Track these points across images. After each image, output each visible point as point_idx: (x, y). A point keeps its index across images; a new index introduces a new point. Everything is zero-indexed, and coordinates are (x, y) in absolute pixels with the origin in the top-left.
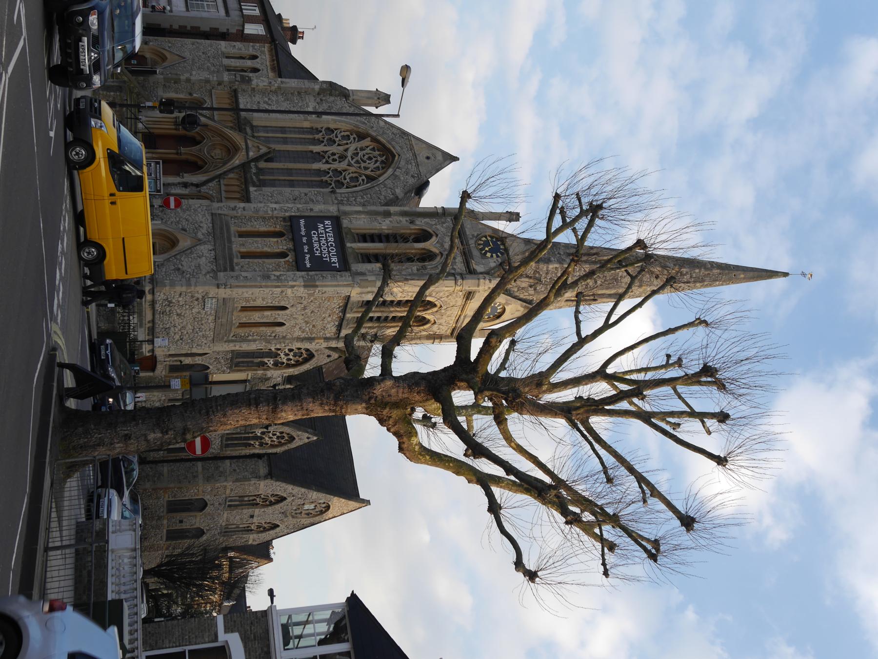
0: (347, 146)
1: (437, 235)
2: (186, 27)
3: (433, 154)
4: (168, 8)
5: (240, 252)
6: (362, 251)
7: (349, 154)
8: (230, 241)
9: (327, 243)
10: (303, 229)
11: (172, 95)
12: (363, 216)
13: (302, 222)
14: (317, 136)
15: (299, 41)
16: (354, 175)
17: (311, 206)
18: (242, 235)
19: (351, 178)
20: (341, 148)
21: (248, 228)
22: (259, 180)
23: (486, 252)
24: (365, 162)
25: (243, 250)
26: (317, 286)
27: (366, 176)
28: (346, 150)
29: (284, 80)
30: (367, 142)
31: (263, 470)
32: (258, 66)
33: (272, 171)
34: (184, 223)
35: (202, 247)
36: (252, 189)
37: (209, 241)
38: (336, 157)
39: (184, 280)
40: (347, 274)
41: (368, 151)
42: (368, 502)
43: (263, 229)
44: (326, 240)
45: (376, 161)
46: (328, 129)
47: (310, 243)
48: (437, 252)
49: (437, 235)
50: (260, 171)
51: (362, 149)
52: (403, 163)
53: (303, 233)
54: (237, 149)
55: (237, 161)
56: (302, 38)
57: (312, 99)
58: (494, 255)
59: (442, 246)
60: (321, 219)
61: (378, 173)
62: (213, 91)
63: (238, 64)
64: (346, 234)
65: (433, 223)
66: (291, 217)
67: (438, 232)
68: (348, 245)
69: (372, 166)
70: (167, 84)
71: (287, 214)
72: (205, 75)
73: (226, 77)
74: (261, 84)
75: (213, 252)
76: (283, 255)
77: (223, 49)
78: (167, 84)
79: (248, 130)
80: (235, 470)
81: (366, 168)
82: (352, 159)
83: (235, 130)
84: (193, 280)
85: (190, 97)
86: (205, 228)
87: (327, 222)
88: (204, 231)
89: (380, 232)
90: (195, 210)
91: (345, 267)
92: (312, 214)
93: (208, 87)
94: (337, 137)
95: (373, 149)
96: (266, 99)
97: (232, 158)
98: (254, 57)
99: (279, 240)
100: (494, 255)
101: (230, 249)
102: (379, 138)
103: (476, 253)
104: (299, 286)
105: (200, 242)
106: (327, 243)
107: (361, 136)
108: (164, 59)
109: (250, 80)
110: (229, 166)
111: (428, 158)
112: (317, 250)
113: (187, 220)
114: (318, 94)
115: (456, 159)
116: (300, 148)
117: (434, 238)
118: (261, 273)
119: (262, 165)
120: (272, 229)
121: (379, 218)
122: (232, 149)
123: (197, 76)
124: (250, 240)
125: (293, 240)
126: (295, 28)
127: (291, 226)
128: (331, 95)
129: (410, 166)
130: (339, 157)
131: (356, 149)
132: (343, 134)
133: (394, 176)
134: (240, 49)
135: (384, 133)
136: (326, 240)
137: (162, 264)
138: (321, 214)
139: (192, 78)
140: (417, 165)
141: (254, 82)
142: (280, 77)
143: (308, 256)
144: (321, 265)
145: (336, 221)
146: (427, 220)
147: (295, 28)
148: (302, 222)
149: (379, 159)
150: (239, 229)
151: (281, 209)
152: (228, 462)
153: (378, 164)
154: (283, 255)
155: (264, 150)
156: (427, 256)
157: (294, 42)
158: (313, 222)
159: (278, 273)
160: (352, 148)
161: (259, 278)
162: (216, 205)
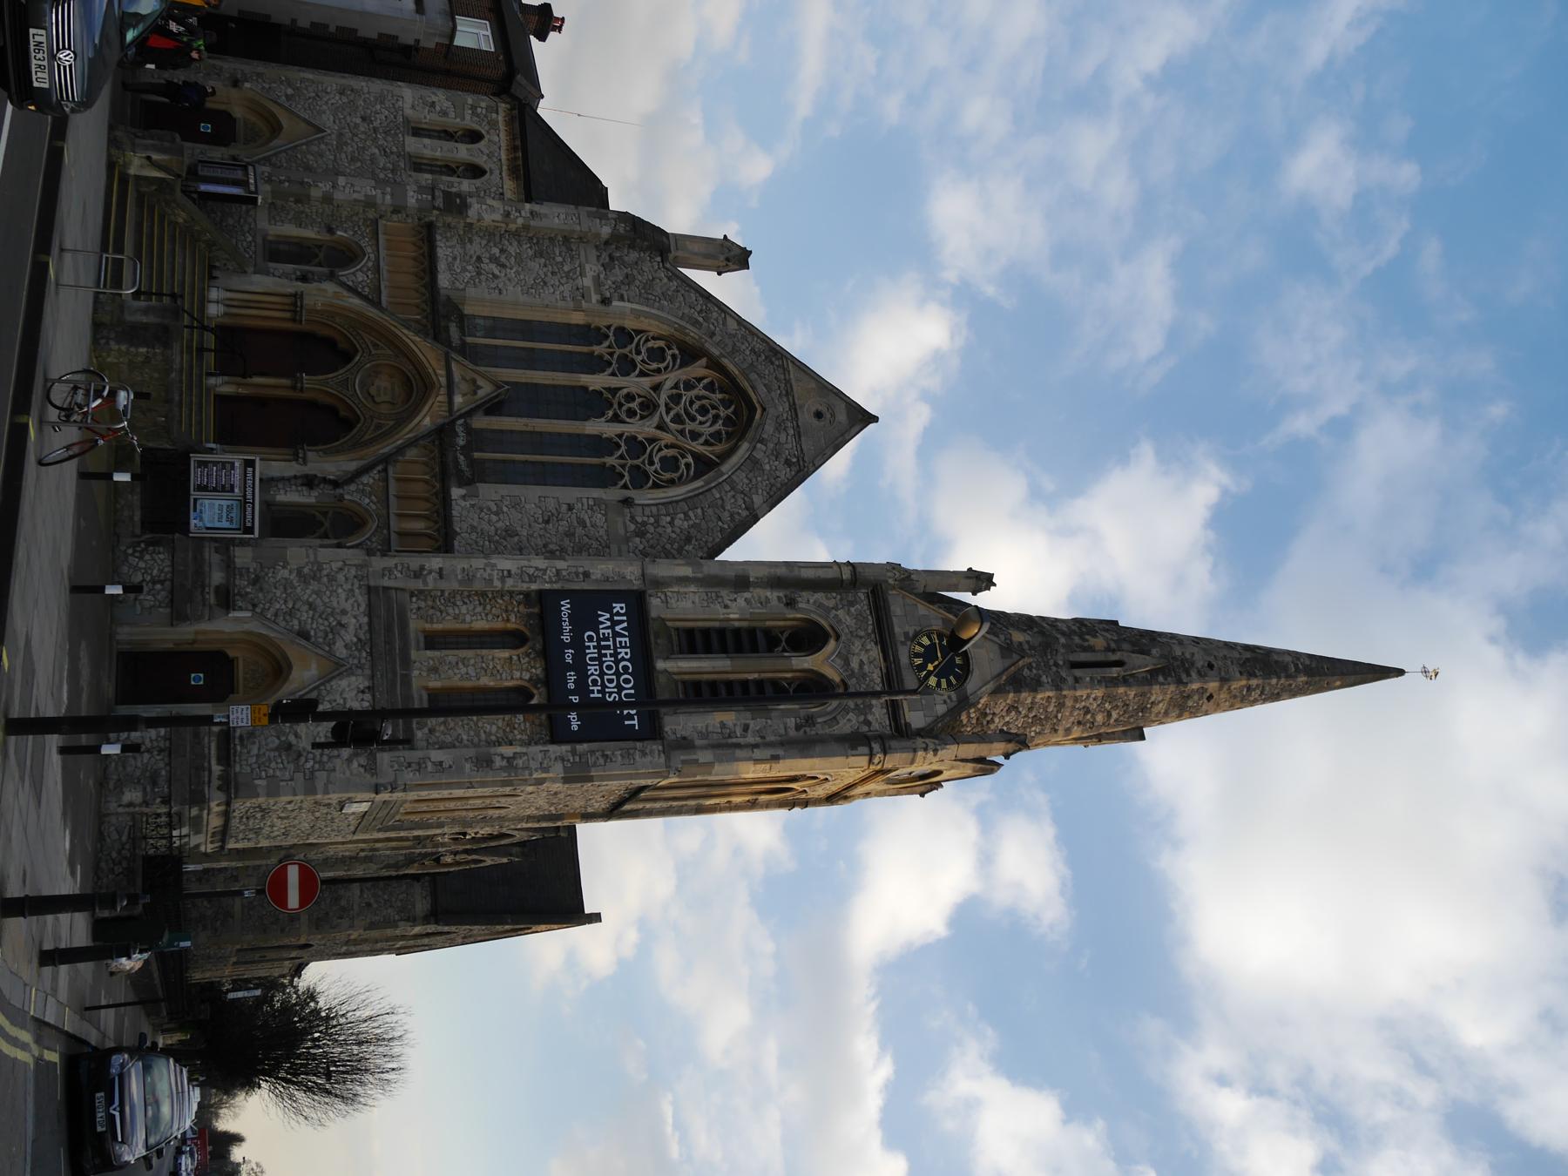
0: (657, 379)
1: (838, 638)
2: (326, 26)
3: (829, 407)
5: (427, 689)
6: (686, 677)
7: (663, 399)
8: (407, 662)
9: (617, 662)
10: (567, 626)
11: (291, 230)
12: (693, 588)
13: (565, 606)
14: (598, 350)
15: (552, 35)
17: (584, 564)
18: (433, 641)
19: (662, 460)
20: (646, 382)
21: (448, 624)
22: (472, 463)
23: (930, 673)
24: (693, 419)
25: (435, 683)
26: (590, 779)
27: (695, 456)
28: (657, 388)
29: (536, 208)
30: (698, 369)
31: (421, 905)
32: (481, 161)
33: (501, 439)
34: (305, 615)
35: (344, 683)
36: (456, 492)
37: (360, 666)
38: (634, 405)
39: (299, 776)
40: (656, 747)
41: (699, 391)
42: (596, 918)
43: (481, 625)
44: (615, 655)
45: (716, 417)
46: (621, 330)
47: (580, 666)
48: (837, 679)
49: (838, 638)
50: (478, 439)
51: (689, 386)
52: (769, 428)
53: (566, 638)
54: (427, 387)
55: (426, 420)
56: (560, 29)
57: (593, 253)
58: (943, 681)
59: (847, 663)
60: (603, 599)
61: (719, 448)
62: (382, 223)
63: (438, 154)
64: (657, 637)
65: (831, 603)
66: (541, 593)
67: (839, 629)
68: (660, 665)
69: (707, 430)
70: (279, 203)
71: (534, 587)
72: (365, 188)
74: (489, 218)
75: (368, 696)
77: (408, 112)
78: (279, 203)
79: (454, 330)
80: (369, 905)
81: (695, 436)
82: (668, 410)
83: (427, 335)
84: (321, 776)
85: (327, 237)
86: (351, 629)
87: (617, 607)
88: (349, 637)
89: (724, 624)
90: (332, 578)
91: (652, 731)
92: (586, 586)
93: (371, 214)
94: (638, 353)
95: (710, 387)
96: (496, 251)
97: (415, 410)
98: (474, 137)
99: (514, 653)
100: (943, 681)
101: (406, 681)
102: (725, 361)
104: (554, 780)
106: (617, 662)
107: (690, 354)
108: (276, 128)
110: (406, 433)
111: (819, 415)
112: (595, 682)
113: (311, 606)
114: (607, 243)
115: (875, 419)
117: (832, 644)
118: (471, 752)
119: (481, 422)
120: (499, 625)
121: (724, 593)
122: (416, 387)
123: (351, 190)
124: (451, 655)
127: (541, 616)
128: (632, 247)
129: (783, 437)
130: (641, 405)
131: (676, 386)
132: (650, 344)
133: (753, 463)
134: (444, 113)
135: (735, 350)
136: (615, 655)
137: (251, 734)
138: (608, 587)
139: (339, 196)
140: (798, 435)
141: (472, 213)
142: (529, 199)
144: (603, 724)
145: (637, 601)
146: (819, 596)
147: (546, 8)
148: (565, 606)
149: (723, 412)
150: (428, 626)
151: (522, 573)
152: (356, 887)
153: (718, 426)
155: (486, 389)
156: (814, 688)
157: (542, 37)
158: (590, 604)
159: (508, 751)
160: (670, 379)
161: (468, 766)
162: (378, 563)
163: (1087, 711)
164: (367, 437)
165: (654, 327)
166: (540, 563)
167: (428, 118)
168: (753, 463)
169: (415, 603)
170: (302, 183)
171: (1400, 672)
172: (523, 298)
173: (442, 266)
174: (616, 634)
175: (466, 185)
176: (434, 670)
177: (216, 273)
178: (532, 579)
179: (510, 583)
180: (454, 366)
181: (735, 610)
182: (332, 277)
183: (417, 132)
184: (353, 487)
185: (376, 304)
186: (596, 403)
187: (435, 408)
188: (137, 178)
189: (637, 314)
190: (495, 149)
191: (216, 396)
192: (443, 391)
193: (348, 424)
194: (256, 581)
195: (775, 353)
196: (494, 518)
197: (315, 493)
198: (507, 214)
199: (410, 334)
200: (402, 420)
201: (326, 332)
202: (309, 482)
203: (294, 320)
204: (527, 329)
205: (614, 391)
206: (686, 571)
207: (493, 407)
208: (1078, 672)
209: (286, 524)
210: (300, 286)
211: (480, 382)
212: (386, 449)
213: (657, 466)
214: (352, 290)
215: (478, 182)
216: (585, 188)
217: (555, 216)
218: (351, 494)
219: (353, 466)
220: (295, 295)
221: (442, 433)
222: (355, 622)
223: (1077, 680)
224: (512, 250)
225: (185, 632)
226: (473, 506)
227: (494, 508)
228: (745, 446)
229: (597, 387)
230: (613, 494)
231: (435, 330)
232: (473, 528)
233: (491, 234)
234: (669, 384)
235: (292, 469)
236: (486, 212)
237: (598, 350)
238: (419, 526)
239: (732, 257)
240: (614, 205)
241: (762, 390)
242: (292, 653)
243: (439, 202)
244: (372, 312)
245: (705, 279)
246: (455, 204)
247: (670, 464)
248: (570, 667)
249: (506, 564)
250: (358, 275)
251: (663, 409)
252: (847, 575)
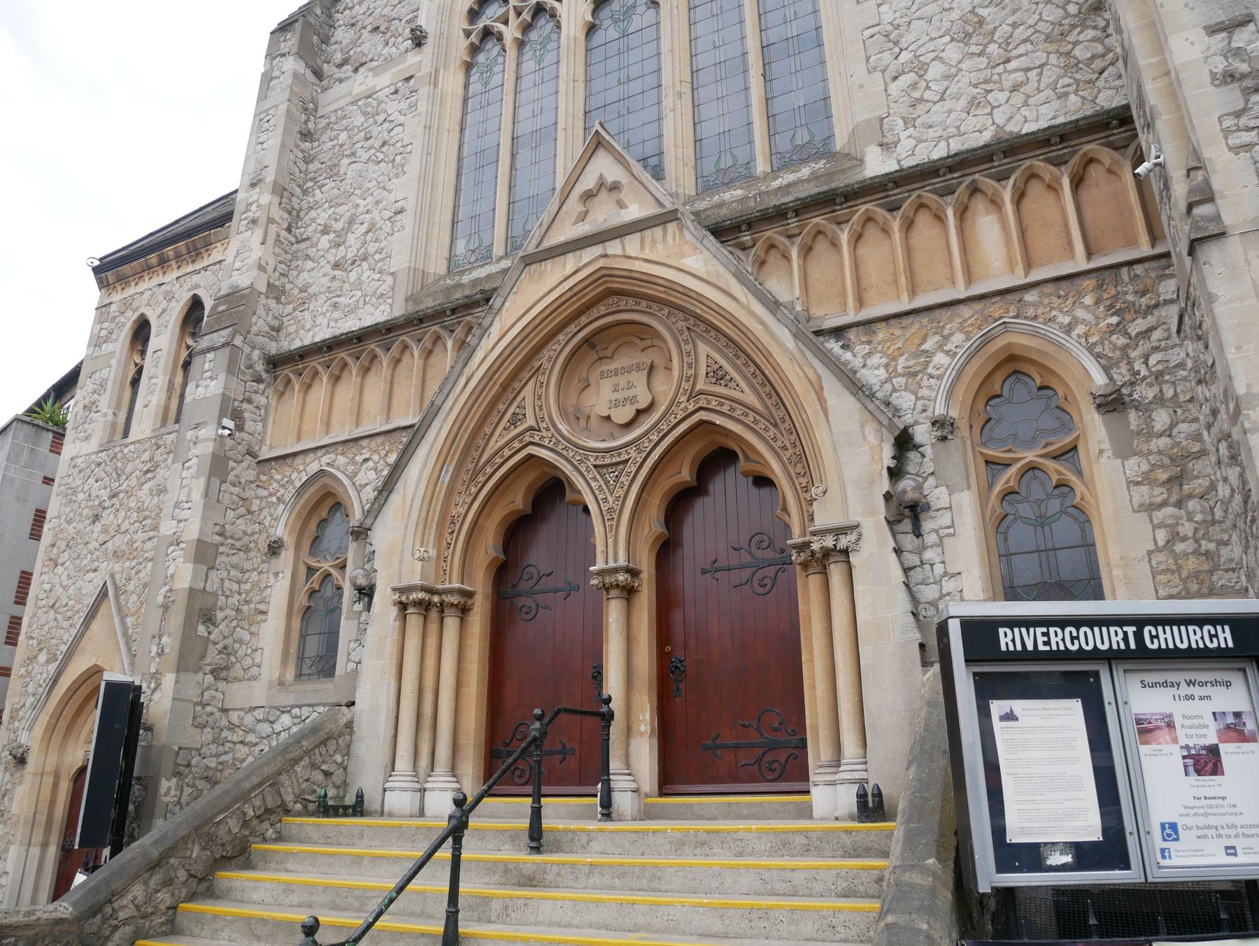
55: (692, 263)
70: (213, 657)
73: (209, 385)
77: (94, 444)
78: (213, 657)
93: (244, 471)
139: (192, 532)
164: (750, 398)
170: (165, 607)
173: (351, 325)
177: (350, 800)
182: (360, 533)
184: (904, 400)
185: (416, 433)
187: (659, 253)
191: (662, 794)
192: (614, 247)
193: (718, 457)
196: (935, 70)
197: (938, 495)
199: (486, 343)
200: (697, 319)
202: (908, 513)
203: (464, 611)
210: (383, 599)
211: (588, 182)
214: (387, 488)
219: (842, 403)
220: (403, 606)
224: (323, 216)
226: (908, 122)
227: (909, 78)
232: (973, 103)
235: (875, 553)
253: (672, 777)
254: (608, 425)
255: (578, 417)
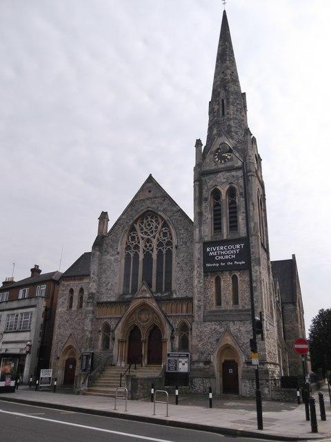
0: (140, 238)
3: (147, 189)
4: (29, 343)
8: (226, 311)
9: (224, 250)
10: (214, 265)
11: (100, 343)
13: (208, 265)
14: (132, 255)
15: (40, 268)
16: (162, 235)
17: (195, 259)
18: (219, 303)
21: (214, 298)
25: (231, 303)
27: (163, 227)
28: (143, 239)
30: (137, 227)
31: (291, 307)
32: (78, 289)
34: (212, 340)
36: (175, 296)
38: (148, 245)
41: (143, 226)
42: (294, 256)
45: (151, 221)
50: (159, 289)
51: (142, 229)
52: (154, 206)
55: (154, 305)
57: (105, 257)
60: (206, 254)
61: (160, 220)
66: (204, 272)
68: (225, 238)
69: (155, 224)
72: (88, 322)
76: (235, 279)
77: (65, 309)
79: (128, 296)
81: (156, 227)
87: (208, 250)
88: (218, 327)
90: (201, 332)
91: (246, 241)
93: (94, 320)
95: (142, 223)
97: (152, 309)
98: (72, 291)
101: (231, 311)
103: (229, 164)
105: (227, 331)
106: (224, 250)
108: (70, 347)
109: (92, 294)
110: (157, 310)
111: (150, 191)
113: (209, 338)
114: (101, 253)
116: (141, 266)
117: (218, 187)
120: (214, 284)
121: (203, 219)
122: (144, 307)
123: (88, 326)
124: (223, 298)
125: (222, 271)
126: (32, 270)
127: (211, 272)
128: (102, 245)
140: (156, 197)
142: (89, 275)
143: (235, 262)
145: (206, 244)
147: (32, 270)
148: (208, 265)
151: (198, 278)
154: (235, 279)
155: (145, 287)
156: (232, 192)
157: (40, 271)
158: (207, 258)
160: (140, 235)
162: (196, 318)
163: (237, 110)
165: (125, 239)
166: (195, 272)
167: (67, 304)
168: (164, 211)
169: (208, 308)
171: (225, 11)
172: (118, 277)
174: (216, 250)
175: (86, 293)
176: (227, 303)
178: (200, 274)
179: (202, 281)
180: (138, 296)
181: (208, 216)
182: (113, 331)
183: (71, 306)
185: (121, 318)
186: (148, 256)
188: (89, 386)
189: (121, 244)
190: (75, 285)
193: (155, 327)
194: (202, 354)
195: (132, 204)
198: (94, 281)
200: (154, 312)
201: (129, 332)
202: (172, 338)
204: (127, 275)
205: (144, 251)
206: (197, 230)
207: (150, 286)
208: (226, 113)
209: (184, 344)
211: (142, 289)
212: (162, 316)
213: (166, 238)
215: (85, 290)
216: (85, 258)
217: (94, 268)
218: (176, 326)
221: (158, 300)
222: (213, 326)
223: (228, 114)
225: (218, 375)
228: (159, 213)
229: (143, 255)
230: (174, 251)
231: (128, 302)
233: (99, 286)
234: (142, 235)
236: (93, 287)
237: (132, 255)
238: (184, 307)
239: (104, 217)
240: (90, 250)
241: (142, 208)
242: (223, 344)
243: (91, 301)
244: (123, 320)
245: (110, 225)
246: (92, 296)
247: (165, 235)
248: (226, 264)
249: (196, 282)
250: (112, 324)
251: (149, 237)
252: (198, 183)
253: (149, 363)
254: (144, 322)
255: (140, 319)
